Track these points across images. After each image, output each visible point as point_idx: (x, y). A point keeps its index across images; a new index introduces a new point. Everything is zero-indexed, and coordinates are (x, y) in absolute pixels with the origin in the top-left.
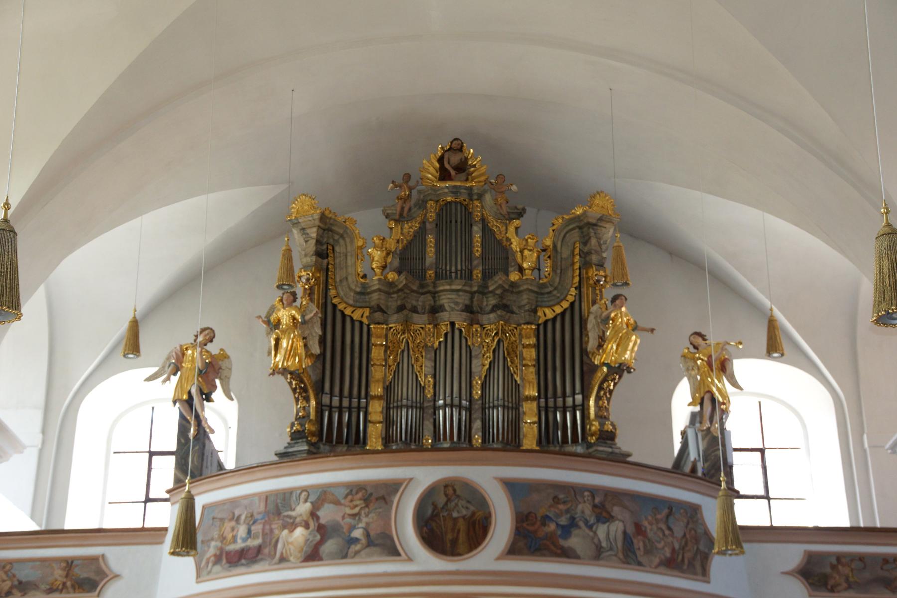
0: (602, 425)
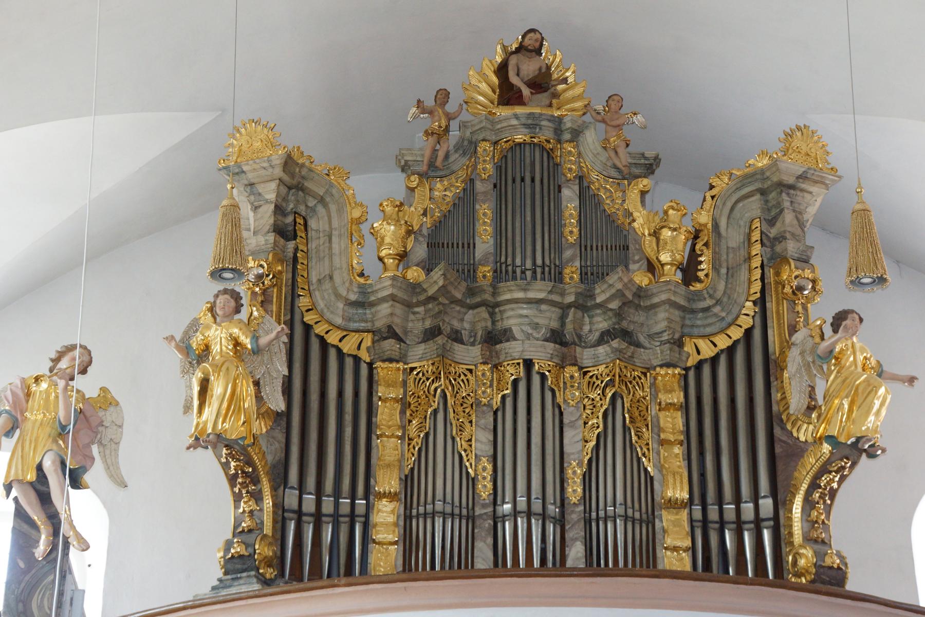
0: (820, 555)
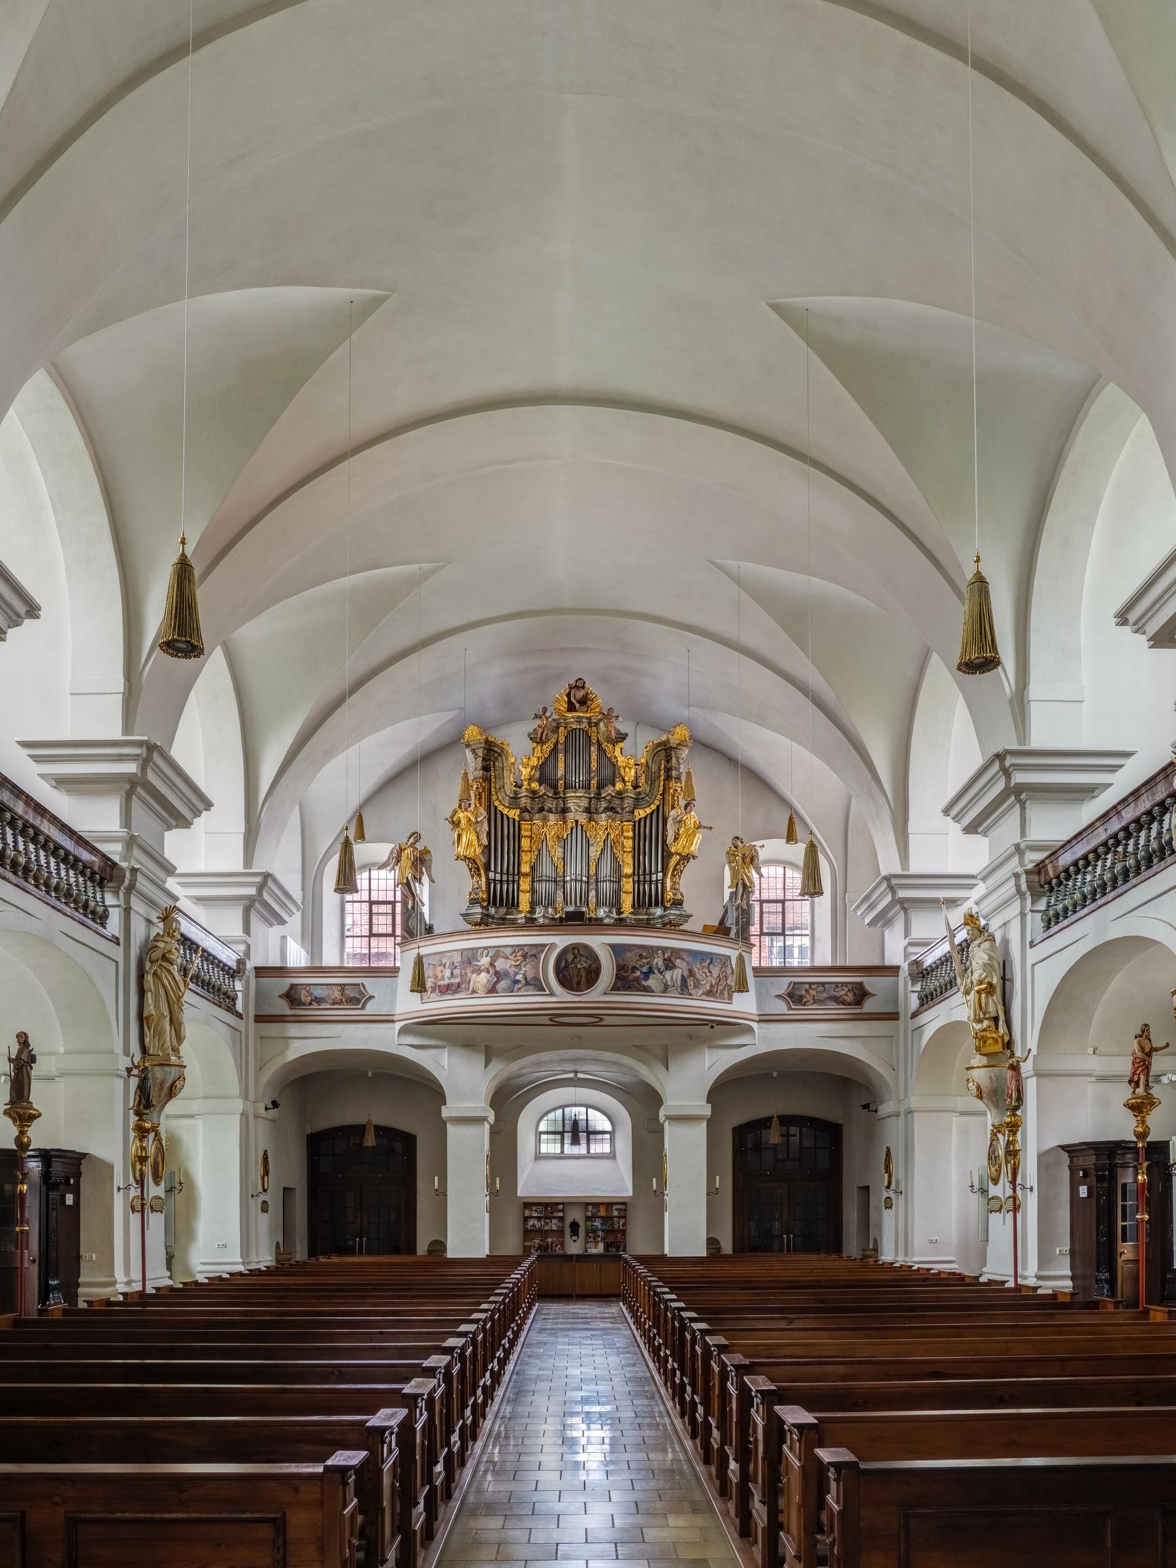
0: (675, 894)
